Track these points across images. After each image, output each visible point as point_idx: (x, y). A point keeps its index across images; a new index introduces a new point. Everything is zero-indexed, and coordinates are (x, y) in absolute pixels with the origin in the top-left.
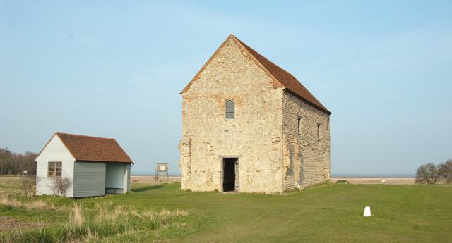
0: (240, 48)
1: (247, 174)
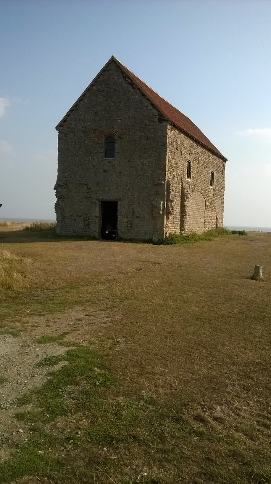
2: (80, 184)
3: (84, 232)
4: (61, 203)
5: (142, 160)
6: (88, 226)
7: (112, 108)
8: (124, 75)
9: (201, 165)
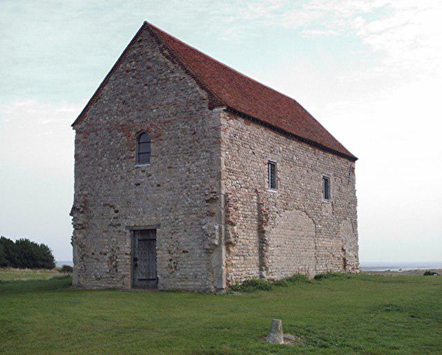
0: (159, 43)
1: (167, 256)
2: (104, 205)
3: (111, 279)
5: (188, 165)
7: (145, 94)
8: (162, 45)
9: (299, 167)
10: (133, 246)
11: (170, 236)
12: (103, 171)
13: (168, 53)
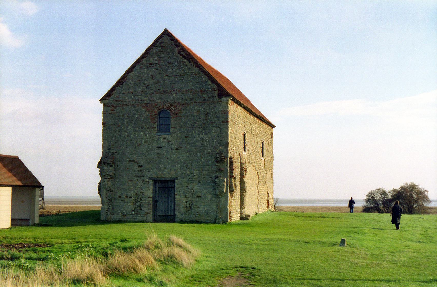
2: (130, 161)
4: (107, 183)
6: (140, 207)
8: (179, 48)
10: (154, 191)
11: (186, 185)
12: (128, 136)
13: (184, 54)
